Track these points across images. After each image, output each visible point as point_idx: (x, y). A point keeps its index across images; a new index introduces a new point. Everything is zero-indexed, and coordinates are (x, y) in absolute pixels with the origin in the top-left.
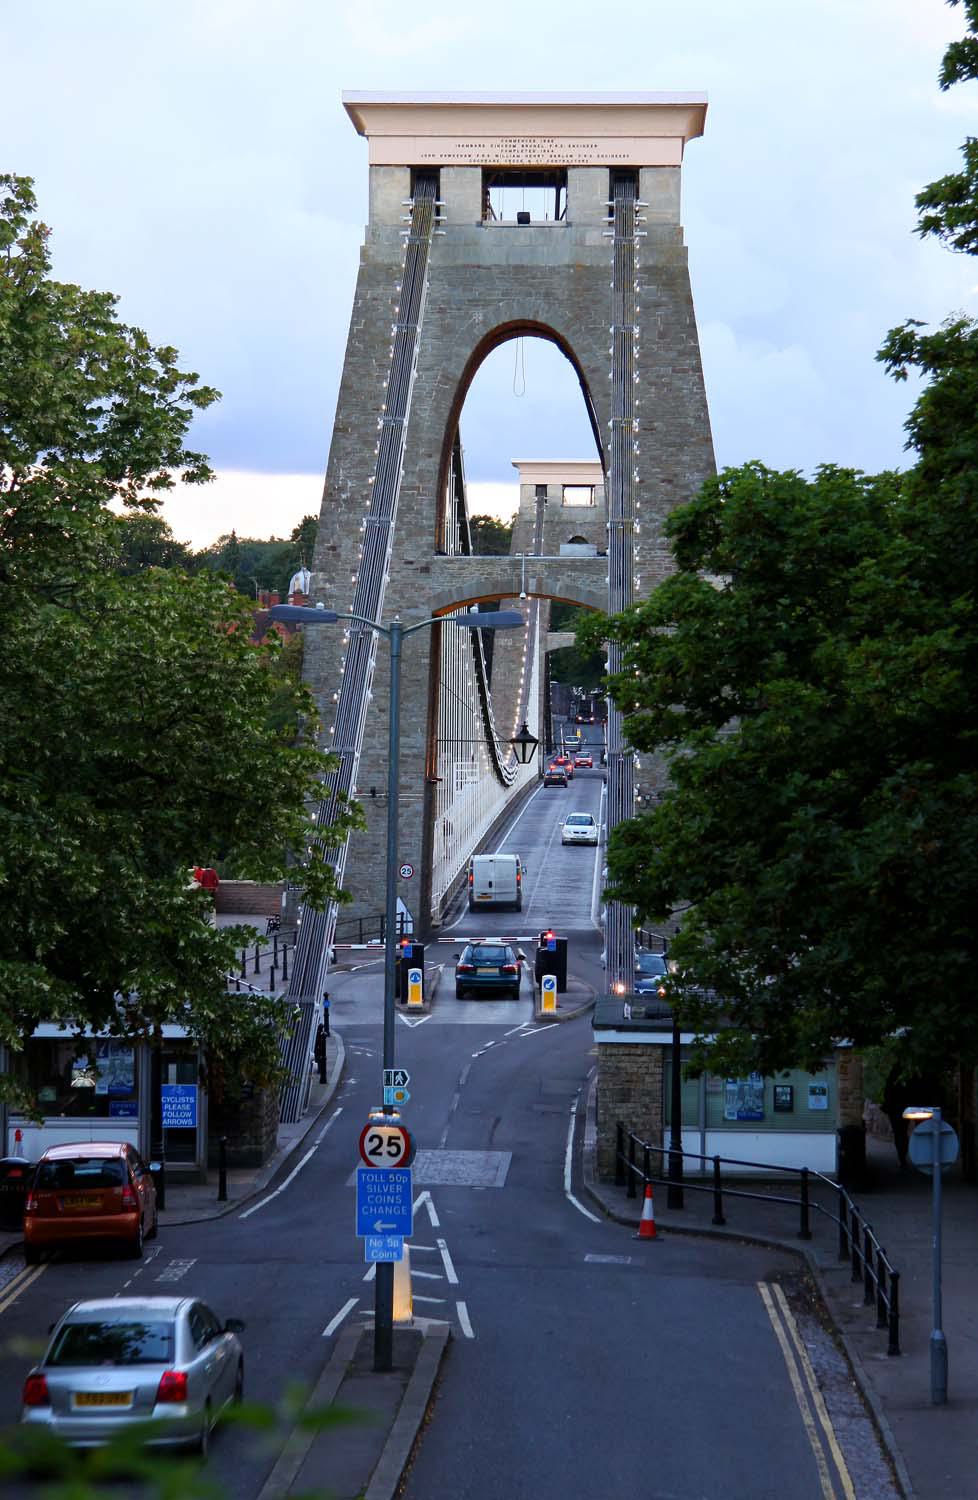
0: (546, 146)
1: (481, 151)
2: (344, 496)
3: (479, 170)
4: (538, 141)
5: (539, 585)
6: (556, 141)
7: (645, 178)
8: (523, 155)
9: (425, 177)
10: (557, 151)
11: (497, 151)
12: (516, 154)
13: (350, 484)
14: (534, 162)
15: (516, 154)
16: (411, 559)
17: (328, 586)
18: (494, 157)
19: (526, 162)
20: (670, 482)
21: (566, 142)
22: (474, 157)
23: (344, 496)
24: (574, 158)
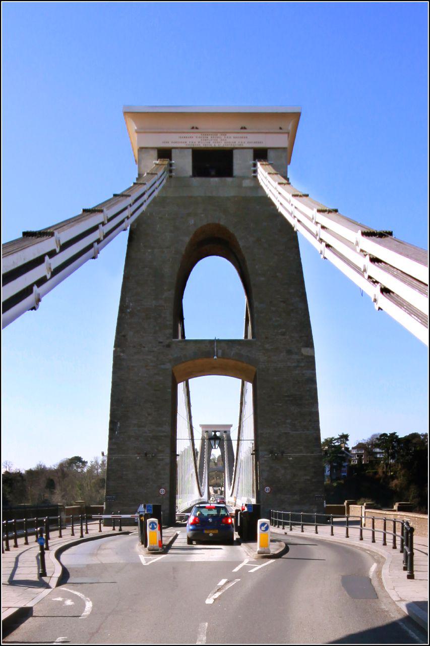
0: (223, 137)
1: (191, 140)
2: (128, 311)
3: (191, 150)
4: (219, 135)
5: (223, 354)
6: (228, 135)
7: (271, 154)
8: (211, 142)
9: (164, 154)
10: (228, 140)
11: (200, 140)
12: (208, 141)
13: (131, 304)
14: (217, 145)
15: (208, 141)
16: (162, 341)
17: (122, 354)
18: (197, 143)
19: (213, 145)
20: (284, 302)
21: (232, 135)
22: (188, 143)
23: (128, 311)
24: (237, 143)
